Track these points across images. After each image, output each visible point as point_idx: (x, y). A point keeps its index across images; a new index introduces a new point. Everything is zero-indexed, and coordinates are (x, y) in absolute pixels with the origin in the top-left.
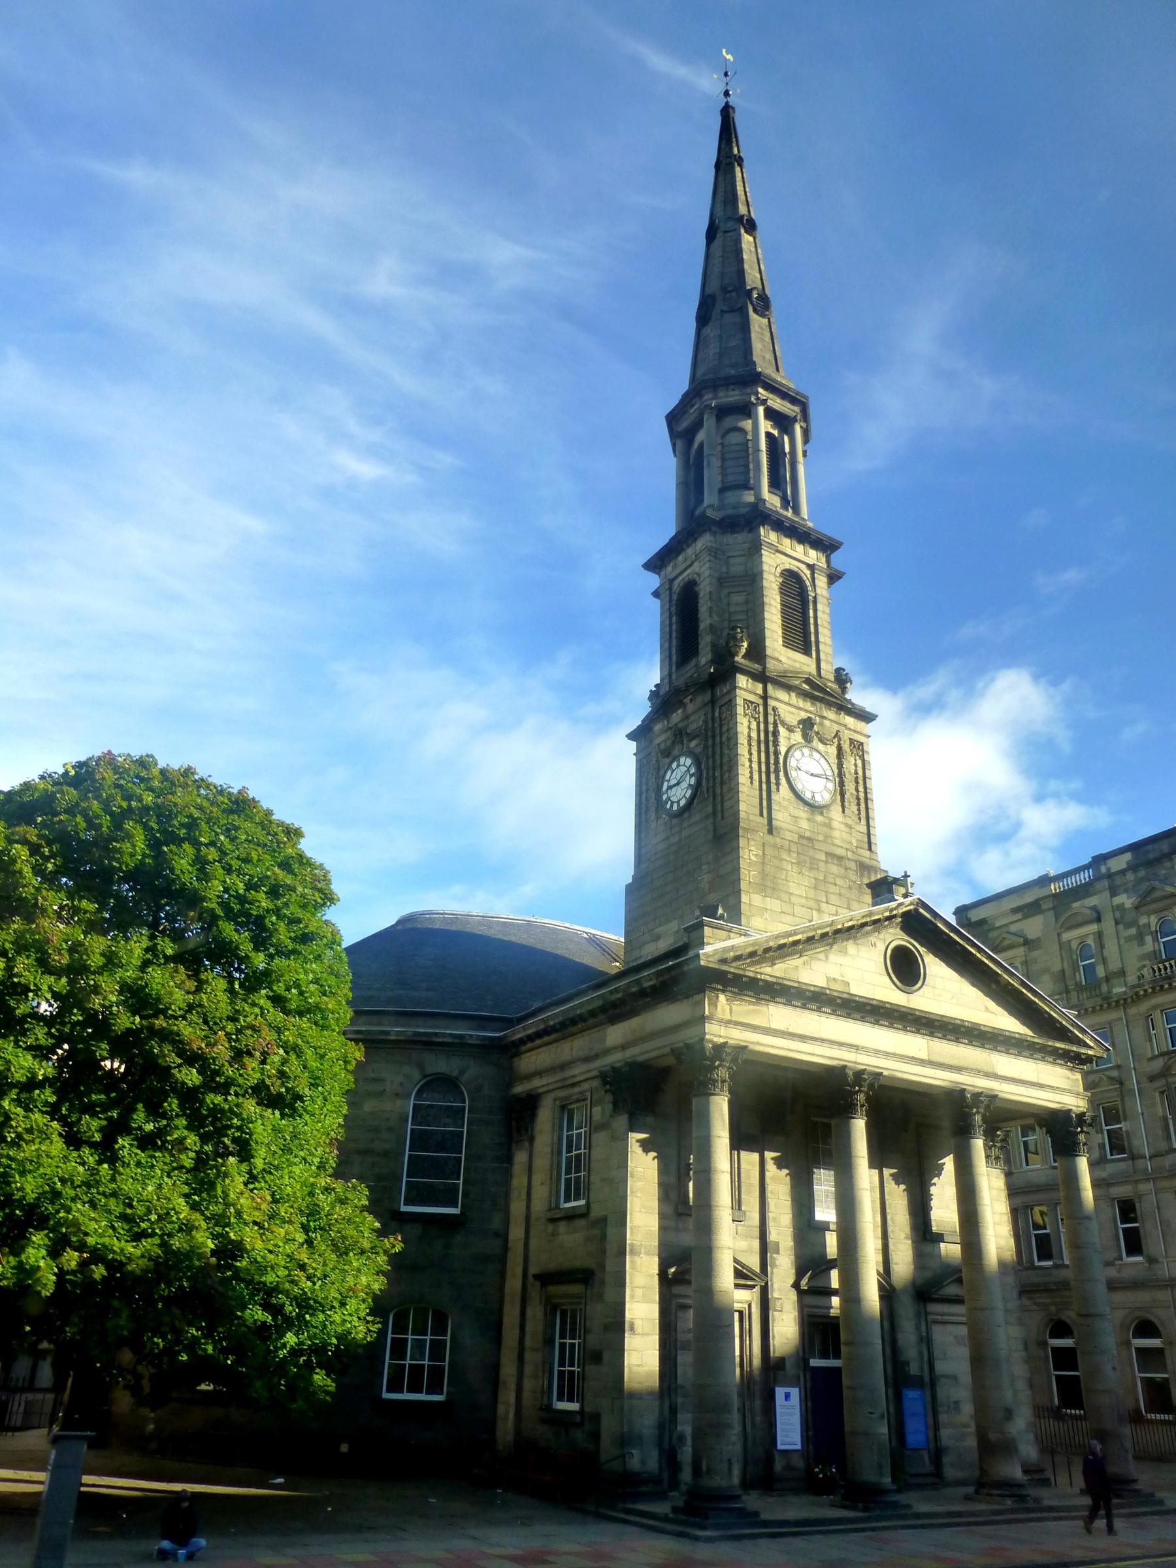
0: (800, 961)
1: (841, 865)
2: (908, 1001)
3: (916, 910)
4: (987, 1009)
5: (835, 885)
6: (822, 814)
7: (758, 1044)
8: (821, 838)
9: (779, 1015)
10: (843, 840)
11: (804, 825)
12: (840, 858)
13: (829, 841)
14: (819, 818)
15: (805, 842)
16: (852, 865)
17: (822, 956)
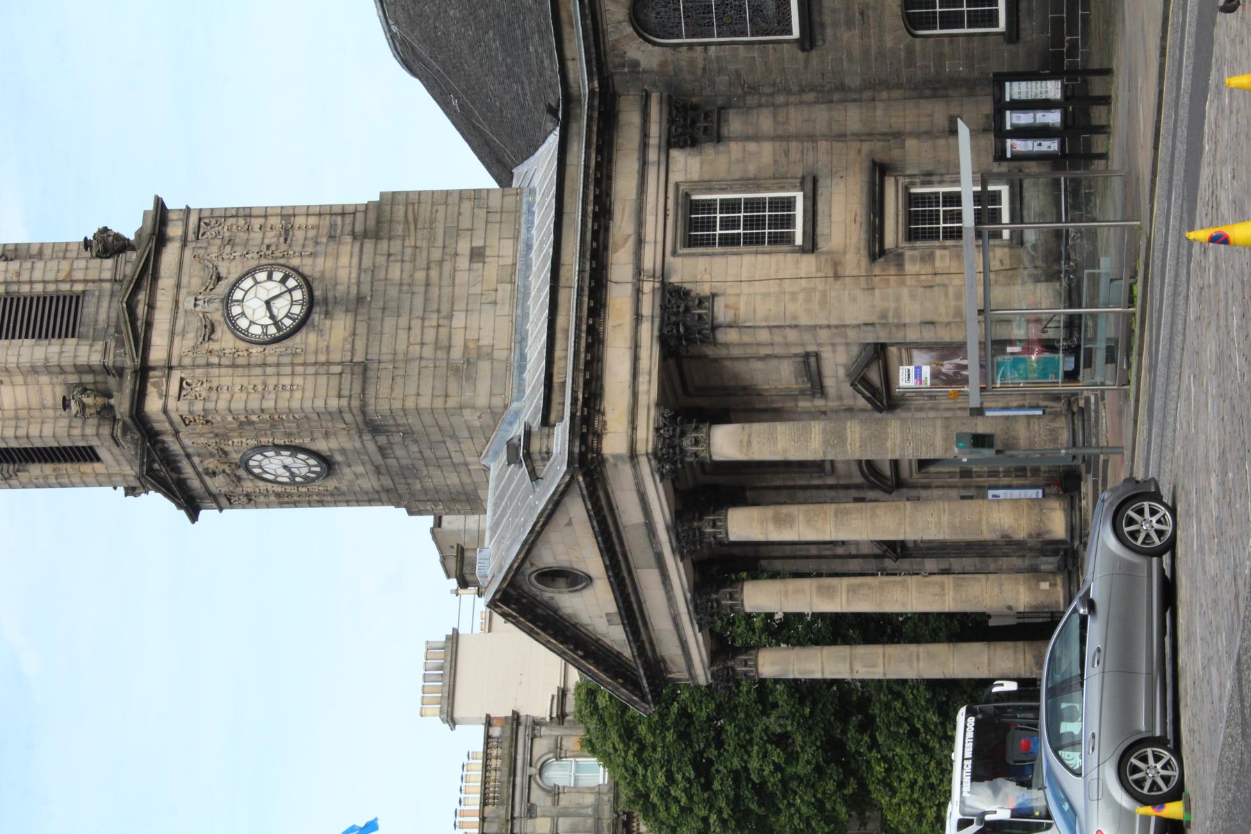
0: (604, 639)
1: (391, 448)
2: (599, 578)
3: (499, 600)
4: (570, 524)
5: (421, 452)
6: (332, 456)
7: (702, 661)
8: (366, 458)
9: (669, 648)
10: (350, 438)
11: (360, 469)
12: (381, 449)
13: (362, 451)
14: (338, 458)
15: (383, 470)
16: (382, 440)
17: (590, 628)
